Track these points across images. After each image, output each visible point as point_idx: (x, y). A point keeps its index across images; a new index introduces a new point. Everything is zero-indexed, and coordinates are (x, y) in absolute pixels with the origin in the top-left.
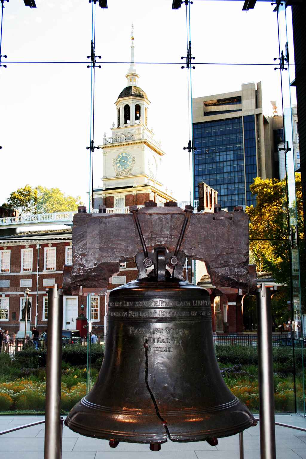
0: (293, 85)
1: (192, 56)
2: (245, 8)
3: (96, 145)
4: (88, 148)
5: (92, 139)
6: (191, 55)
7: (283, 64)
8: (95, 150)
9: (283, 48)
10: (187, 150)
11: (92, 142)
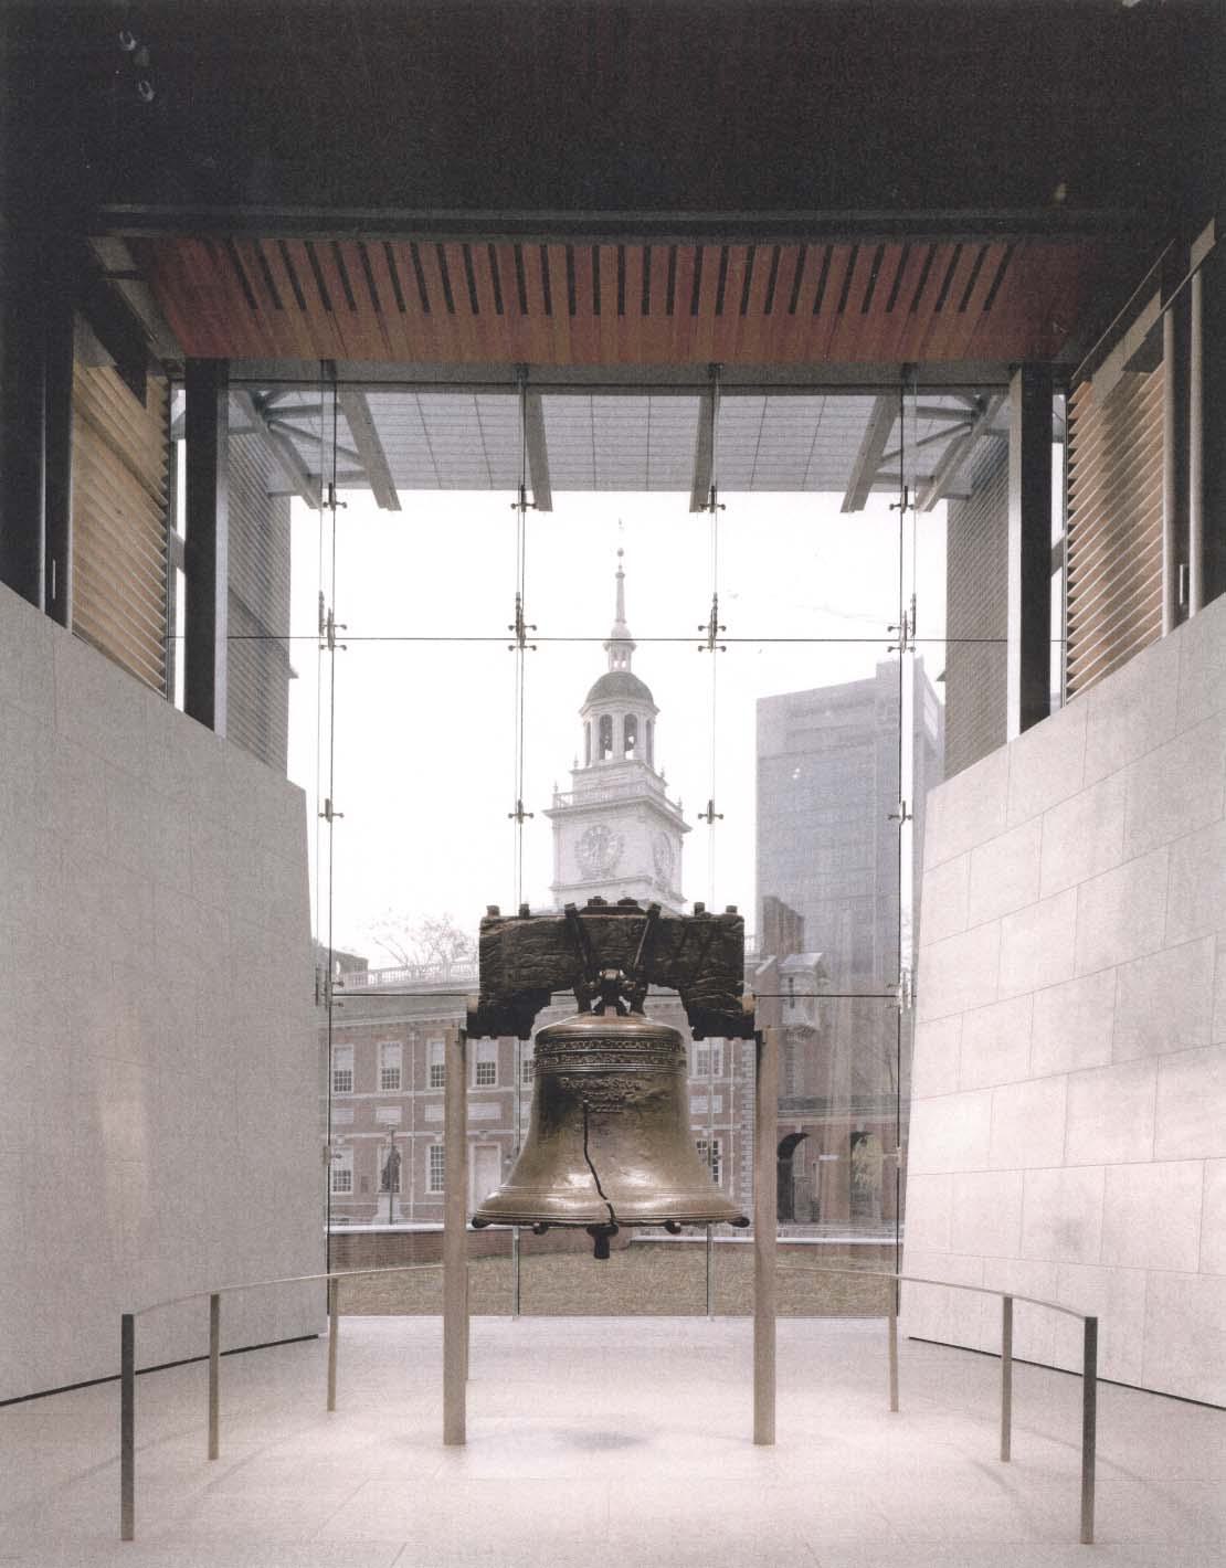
0: (941, 678)
1: (718, 625)
2: (845, 509)
3: (526, 810)
4: (511, 816)
5: (519, 798)
6: (716, 622)
7: (906, 639)
8: (526, 818)
9: (907, 606)
10: (705, 819)
11: (520, 805)
